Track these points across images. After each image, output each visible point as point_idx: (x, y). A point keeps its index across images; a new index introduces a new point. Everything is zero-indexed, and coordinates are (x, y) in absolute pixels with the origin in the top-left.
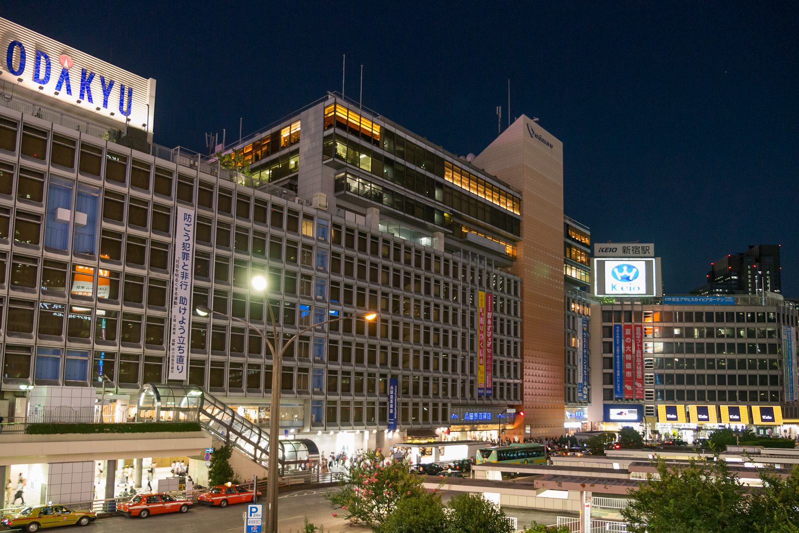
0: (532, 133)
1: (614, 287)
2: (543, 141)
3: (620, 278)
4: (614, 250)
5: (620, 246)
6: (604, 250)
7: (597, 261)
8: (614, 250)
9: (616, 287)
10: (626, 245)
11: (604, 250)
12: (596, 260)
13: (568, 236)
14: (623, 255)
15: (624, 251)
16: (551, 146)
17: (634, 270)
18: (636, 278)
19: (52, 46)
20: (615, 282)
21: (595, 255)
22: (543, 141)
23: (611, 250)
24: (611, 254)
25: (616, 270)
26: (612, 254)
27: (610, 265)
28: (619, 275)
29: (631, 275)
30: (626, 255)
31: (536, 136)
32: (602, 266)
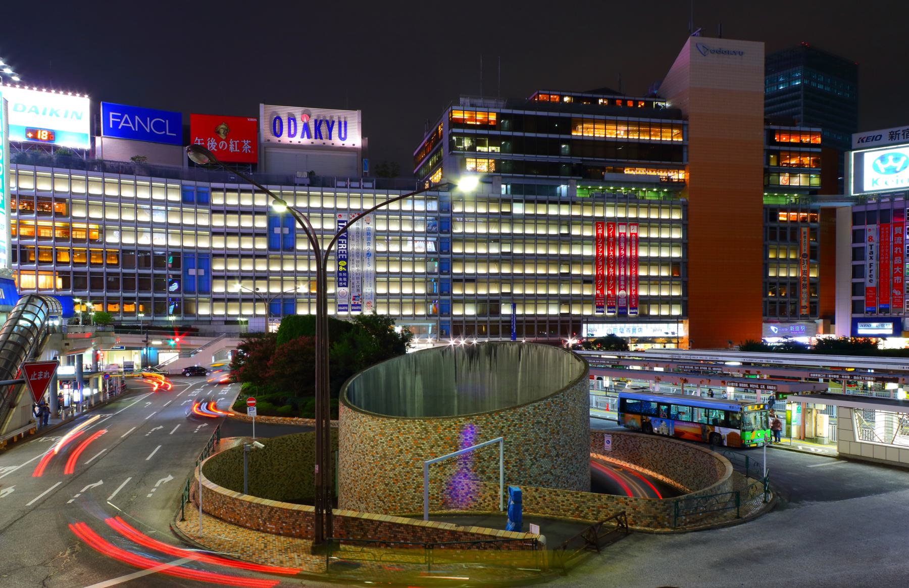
0: (705, 51)
1: (875, 182)
2: (728, 52)
3: (883, 171)
4: (878, 138)
5: (885, 133)
6: (865, 140)
7: (855, 153)
8: (878, 138)
9: (878, 182)
10: (894, 130)
11: (865, 140)
12: (853, 152)
13: (771, 141)
14: (890, 142)
15: (892, 138)
16: (741, 54)
17: (903, 159)
18: (905, 168)
19: (297, 112)
20: (876, 175)
21: (853, 148)
22: (728, 52)
23: (875, 138)
24: (875, 143)
25: (879, 163)
26: (876, 143)
27: (871, 157)
28: (882, 166)
29: (899, 165)
30: (894, 141)
31: (713, 52)
32: (859, 159)
